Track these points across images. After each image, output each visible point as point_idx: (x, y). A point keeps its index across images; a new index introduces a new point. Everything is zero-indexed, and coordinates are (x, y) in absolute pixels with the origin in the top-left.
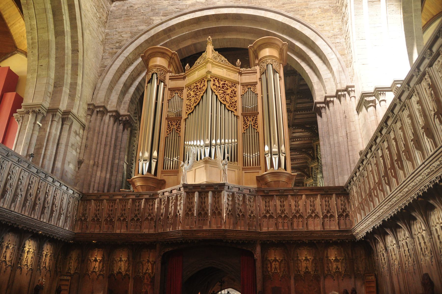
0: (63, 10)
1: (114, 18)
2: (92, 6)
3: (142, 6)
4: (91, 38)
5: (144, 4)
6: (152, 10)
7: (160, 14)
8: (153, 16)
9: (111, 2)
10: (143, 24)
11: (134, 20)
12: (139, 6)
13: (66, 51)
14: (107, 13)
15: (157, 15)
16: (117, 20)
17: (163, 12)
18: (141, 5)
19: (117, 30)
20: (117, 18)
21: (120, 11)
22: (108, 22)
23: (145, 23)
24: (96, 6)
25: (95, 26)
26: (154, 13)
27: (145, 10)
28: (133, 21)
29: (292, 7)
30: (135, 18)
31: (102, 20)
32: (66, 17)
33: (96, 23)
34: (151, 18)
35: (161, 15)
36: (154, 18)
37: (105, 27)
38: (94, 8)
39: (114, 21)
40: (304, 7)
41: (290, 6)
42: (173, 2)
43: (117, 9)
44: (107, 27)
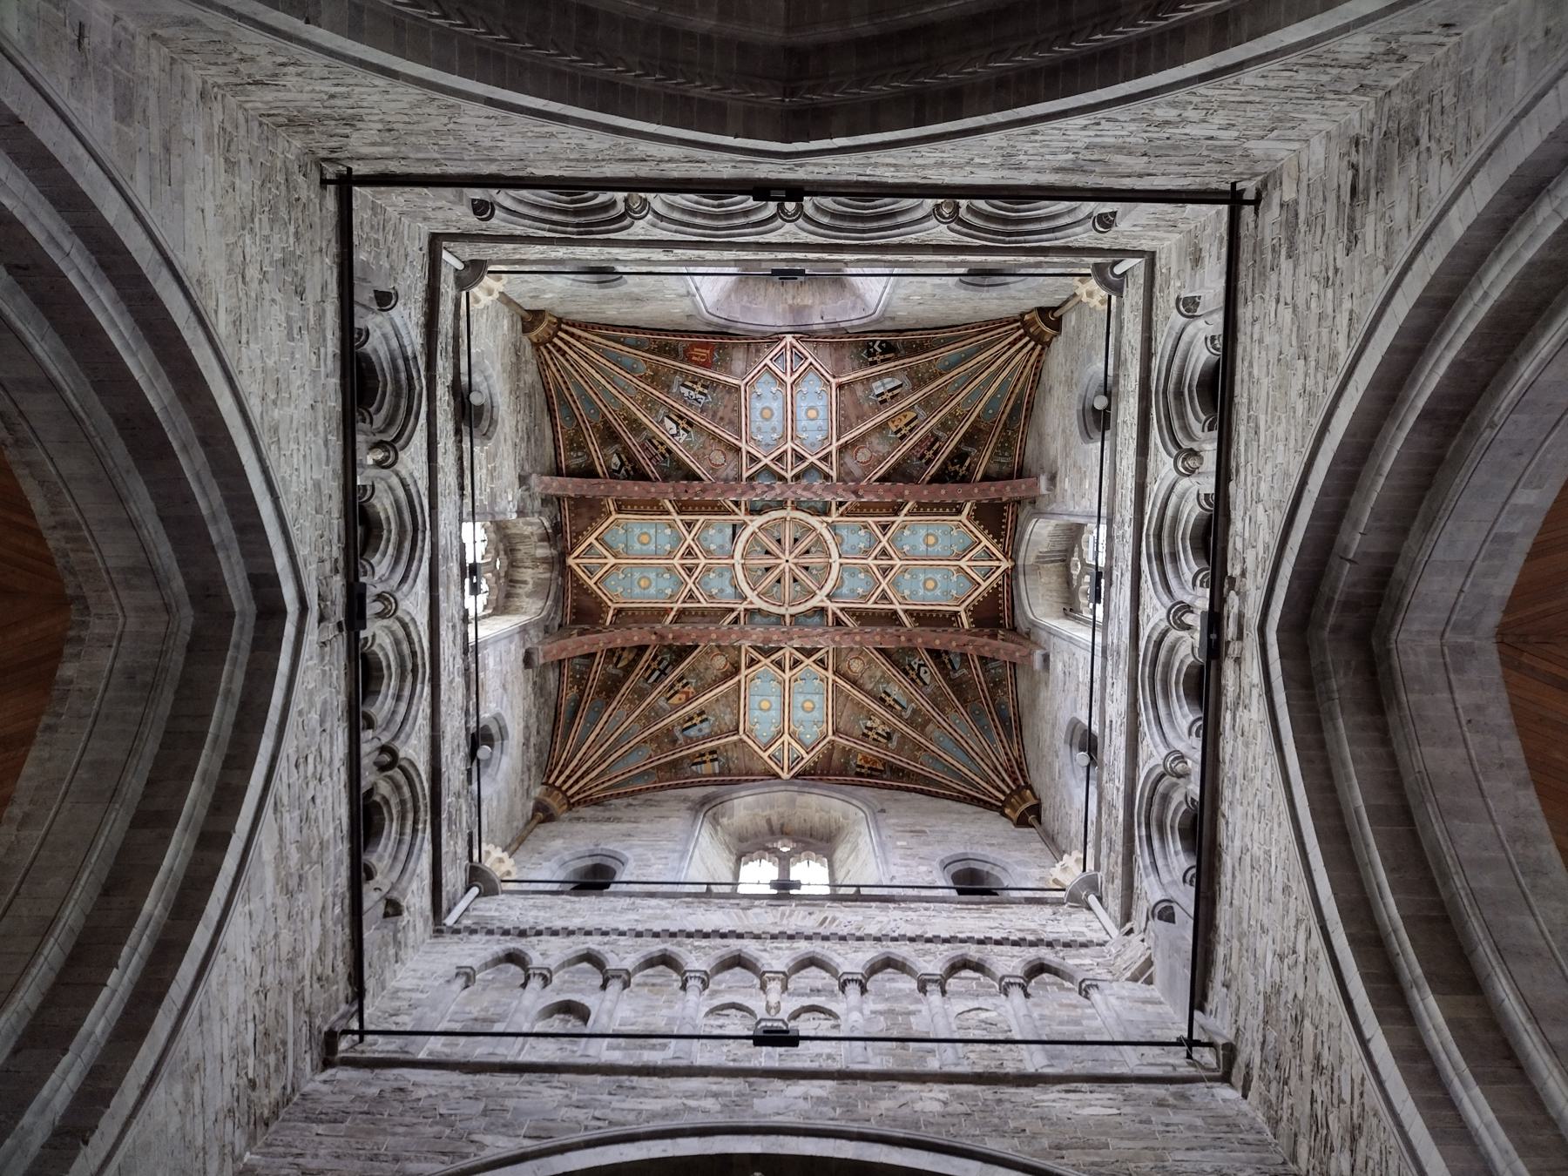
0: (126, 950)
1: (307, 1119)
2: (246, 1009)
3: (445, 1095)
4: (172, 1129)
5: (458, 1087)
6: (485, 1113)
7: (521, 1126)
8: (487, 1131)
9: (320, 1065)
10: (429, 1155)
11: (394, 1134)
12: (434, 1093)
13: (27, 1119)
14: (284, 1088)
15: (503, 1130)
16: (320, 1129)
17: (533, 1124)
18: (441, 1091)
19: (300, 1161)
20: (322, 1122)
21: (345, 1098)
22: (272, 1128)
23: (444, 1154)
24: (261, 1028)
25: (220, 1098)
26: (492, 1124)
27: (456, 1106)
28: (389, 1138)
29: (1097, 1159)
30: (401, 1130)
31: (254, 1095)
32: (120, 982)
33: (228, 1090)
34: (475, 1137)
35: (523, 1132)
36: (488, 1139)
37: (252, 1138)
38: (251, 1025)
39: (303, 1129)
40: (1152, 1165)
41: (1088, 1155)
42: (582, 1097)
43: (336, 1089)
44: (259, 1143)
